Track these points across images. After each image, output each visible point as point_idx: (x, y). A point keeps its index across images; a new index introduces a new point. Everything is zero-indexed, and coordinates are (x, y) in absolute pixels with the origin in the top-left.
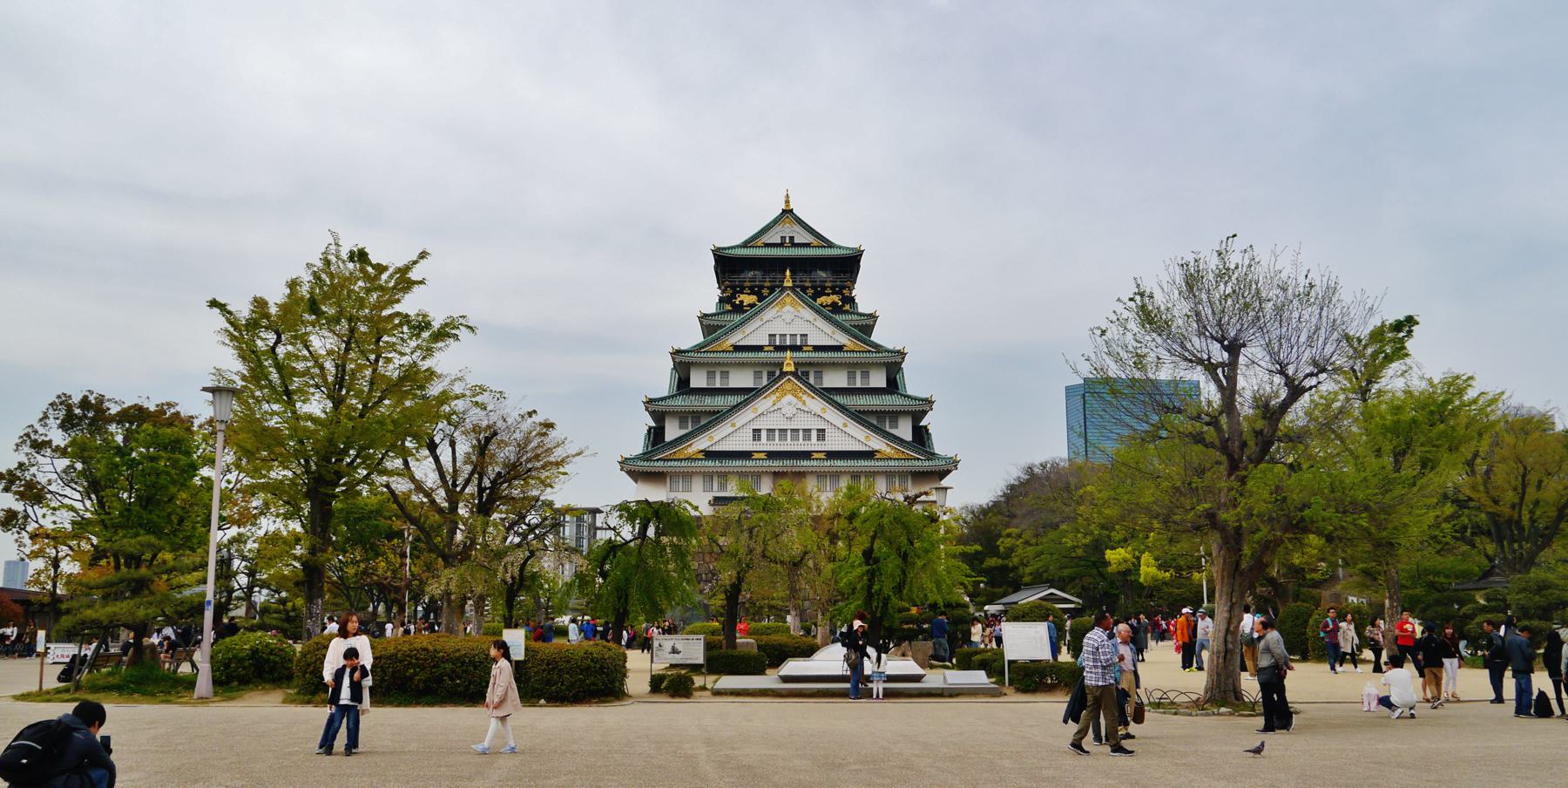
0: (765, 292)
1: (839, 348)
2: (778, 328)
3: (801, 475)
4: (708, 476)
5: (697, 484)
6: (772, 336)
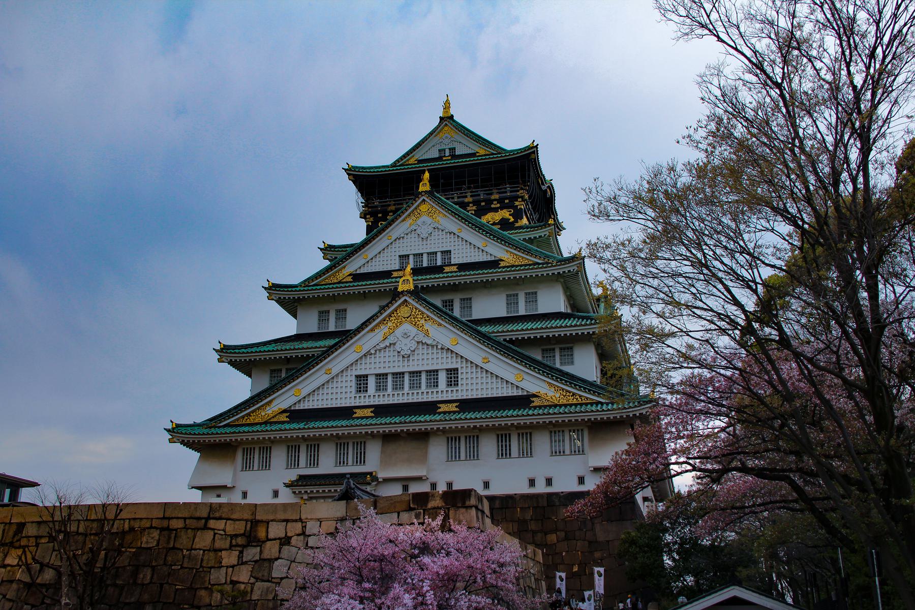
1: (494, 264)
2: (411, 246)
3: (423, 437)
4: (292, 446)
5: (279, 457)
6: (404, 258)
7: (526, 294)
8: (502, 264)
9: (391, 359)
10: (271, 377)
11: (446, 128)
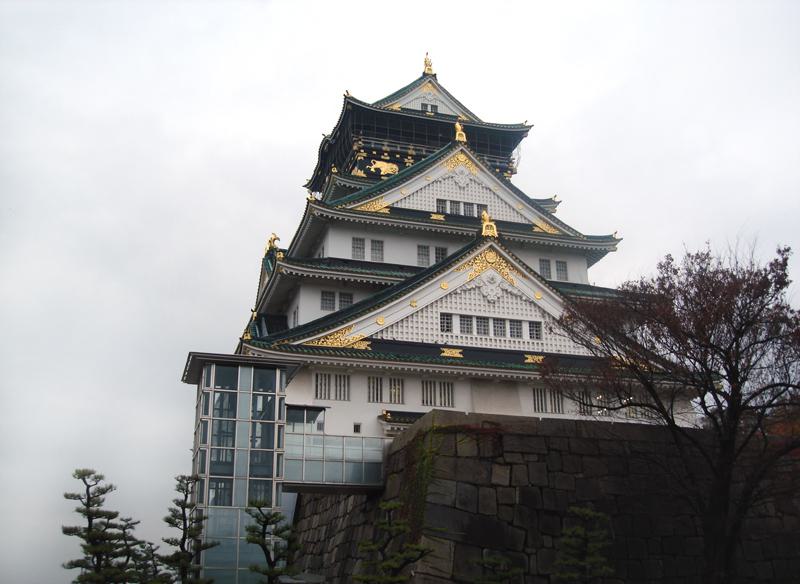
0: (409, 162)
1: (528, 228)
2: (449, 193)
4: (375, 379)
5: (359, 389)
6: (441, 202)
7: (557, 262)
8: (536, 229)
9: (478, 302)
10: (323, 299)
11: (430, 85)
